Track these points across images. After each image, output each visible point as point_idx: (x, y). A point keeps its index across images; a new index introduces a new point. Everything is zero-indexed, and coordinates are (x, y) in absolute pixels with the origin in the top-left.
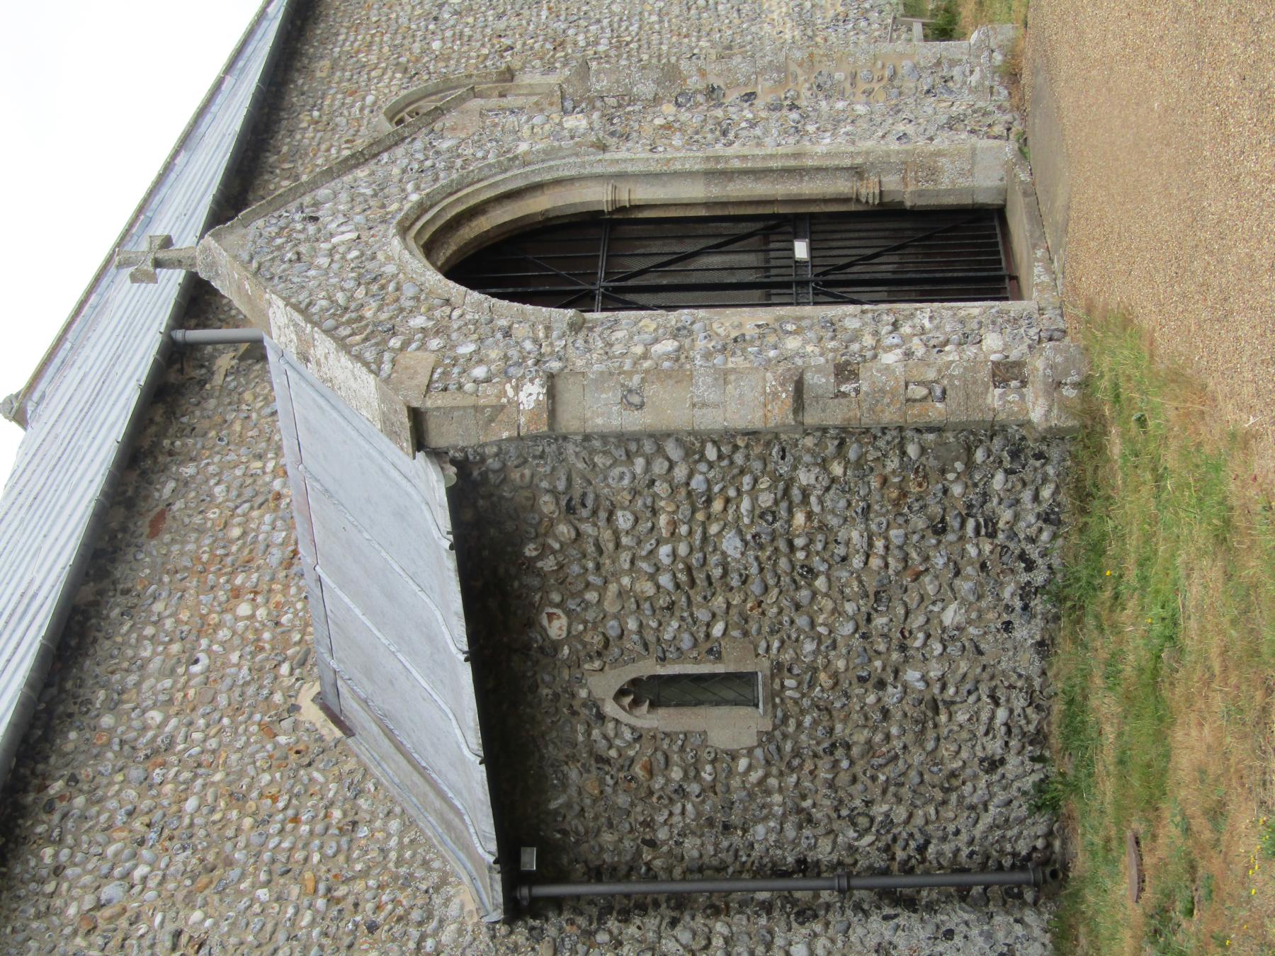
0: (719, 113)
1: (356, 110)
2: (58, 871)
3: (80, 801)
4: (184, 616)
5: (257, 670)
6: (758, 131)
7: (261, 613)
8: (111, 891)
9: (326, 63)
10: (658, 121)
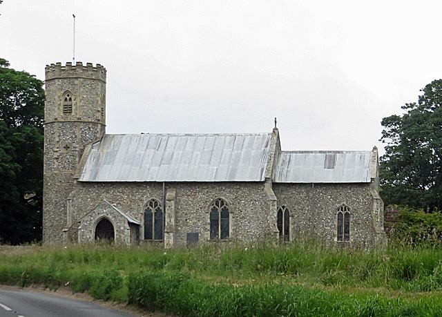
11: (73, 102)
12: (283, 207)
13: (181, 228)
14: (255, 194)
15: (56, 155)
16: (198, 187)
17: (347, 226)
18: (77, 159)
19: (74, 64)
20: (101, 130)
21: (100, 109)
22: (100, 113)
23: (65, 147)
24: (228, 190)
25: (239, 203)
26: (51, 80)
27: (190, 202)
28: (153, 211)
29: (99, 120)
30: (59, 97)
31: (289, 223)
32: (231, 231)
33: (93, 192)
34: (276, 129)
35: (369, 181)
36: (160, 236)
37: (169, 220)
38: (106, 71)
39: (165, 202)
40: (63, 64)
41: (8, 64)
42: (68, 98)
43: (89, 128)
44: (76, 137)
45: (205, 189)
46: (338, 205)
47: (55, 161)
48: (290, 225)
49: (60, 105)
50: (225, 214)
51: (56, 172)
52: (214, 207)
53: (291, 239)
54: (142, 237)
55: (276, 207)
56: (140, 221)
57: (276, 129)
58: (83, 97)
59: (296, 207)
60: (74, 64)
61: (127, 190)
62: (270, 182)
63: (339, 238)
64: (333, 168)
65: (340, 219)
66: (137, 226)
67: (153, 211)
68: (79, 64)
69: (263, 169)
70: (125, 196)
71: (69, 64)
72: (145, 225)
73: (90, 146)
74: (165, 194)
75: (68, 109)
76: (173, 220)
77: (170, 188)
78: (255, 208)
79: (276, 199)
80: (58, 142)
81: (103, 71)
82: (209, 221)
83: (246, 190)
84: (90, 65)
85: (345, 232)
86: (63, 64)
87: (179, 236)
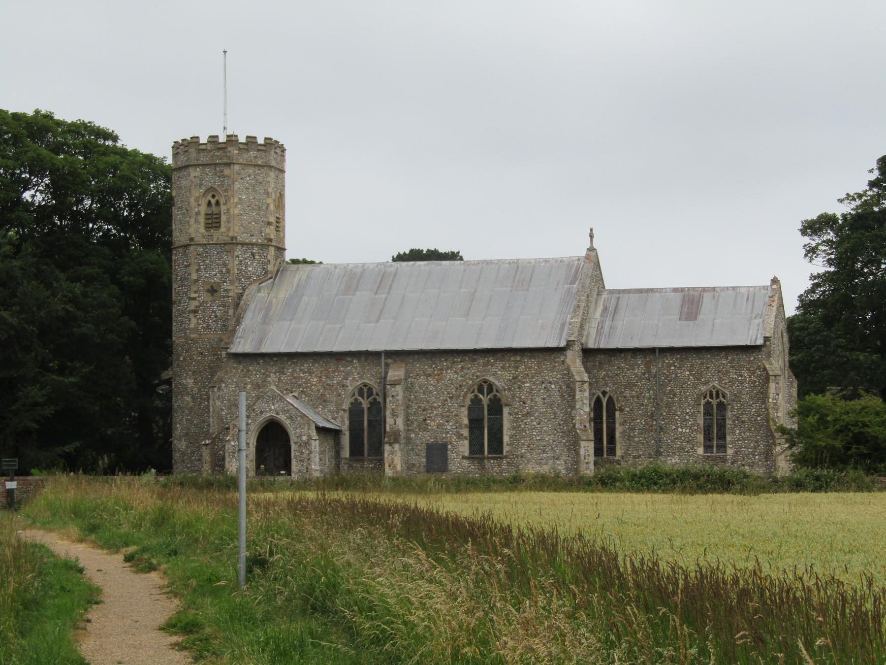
0: (306, 460)
1: (494, 370)
2: (259, 364)
3: (272, 363)
4: (314, 370)
5: (301, 384)
6: (300, 466)
7: (314, 383)
8: (254, 372)
9: (518, 358)
10: (304, 451)
11: (223, 208)
12: (604, 393)
13: (417, 435)
14: (550, 373)
15: (193, 305)
16: (446, 360)
17: (722, 426)
18: (231, 312)
19: (222, 139)
20: (276, 258)
21: (272, 219)
22: (272, 227)
24: (500, 364)
25: (520, 387)
27: (431, 388)
28: (365, 404)
29: (270, 240)
30: (197, 200)
31: (614, 422)
32: (506, 439)
33: (256, 372)
34: (591, 249)
35: (760, 342)
36: (377, 451)
37: (394, 422)
38: (284, 150)
39: (385, 388)
40: (203, 140)
41: (115, 139)
42: (213, 201)
43: (253, 255)
44: (228, 271)
45: (457, 362)
46: (703, 388)
47: (192, 316)
48: (617, 425)
49: (198, 214)
50: (496, 407)
51: (193, 336)
52: (476, 396)
53: (619, 452)
54: (346, 453)
55: (587, 394)
56: (342, 423)
57: (591, 249)
58: (240, 199)
59: (627, 393)
60: (222, 139)
61: (317, 368)
62: (577, 347)
63: (708, 448)
64: (695, 319)
65: (708, 413)
66: (335, 434)
67: (365, 404)
68: (232, 140)
69: (563, 325)
70: (313, 376)
71: (213, 139)
72: (352, 430)
73: (254, 287)
74: (386, 373)
75: (213, 221)
76: (400, 422)
77: (395, 362)
78: (549, 396)
79: (586, 379)
80: (196, 281)
81: (278, 151)
82: (466, 421)
83: (533, 363)
84: (251, 140)
85: (719, 438)
86: (203, 140)
87: (412, 450)
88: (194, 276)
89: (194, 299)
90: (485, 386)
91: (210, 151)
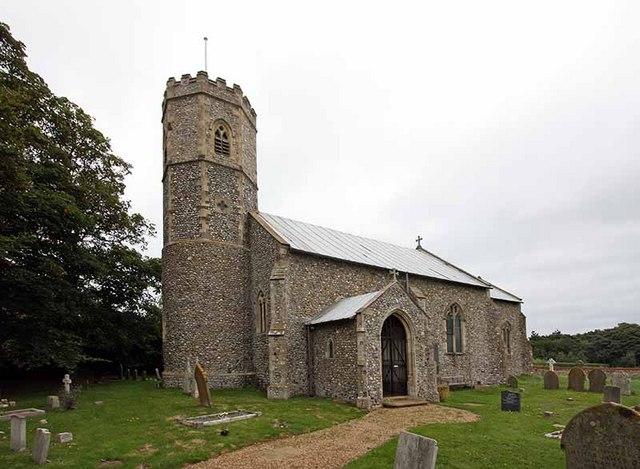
15: (205, 213)
23: (219, 205)
26: (185, 97)
42: (222, 132)
44: (237, 193)
47: (203, 222)
88: (206, 188)
89: (207, 208)
90: (454, 306)
91: (220, 89)
